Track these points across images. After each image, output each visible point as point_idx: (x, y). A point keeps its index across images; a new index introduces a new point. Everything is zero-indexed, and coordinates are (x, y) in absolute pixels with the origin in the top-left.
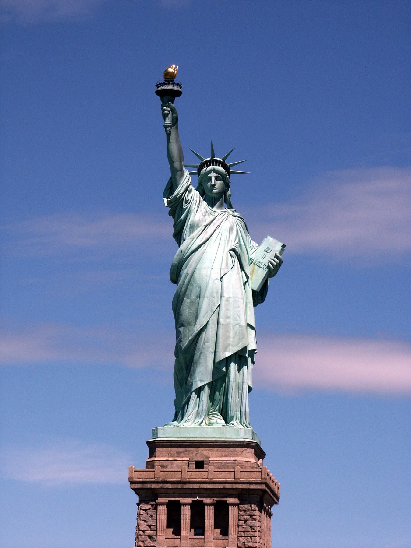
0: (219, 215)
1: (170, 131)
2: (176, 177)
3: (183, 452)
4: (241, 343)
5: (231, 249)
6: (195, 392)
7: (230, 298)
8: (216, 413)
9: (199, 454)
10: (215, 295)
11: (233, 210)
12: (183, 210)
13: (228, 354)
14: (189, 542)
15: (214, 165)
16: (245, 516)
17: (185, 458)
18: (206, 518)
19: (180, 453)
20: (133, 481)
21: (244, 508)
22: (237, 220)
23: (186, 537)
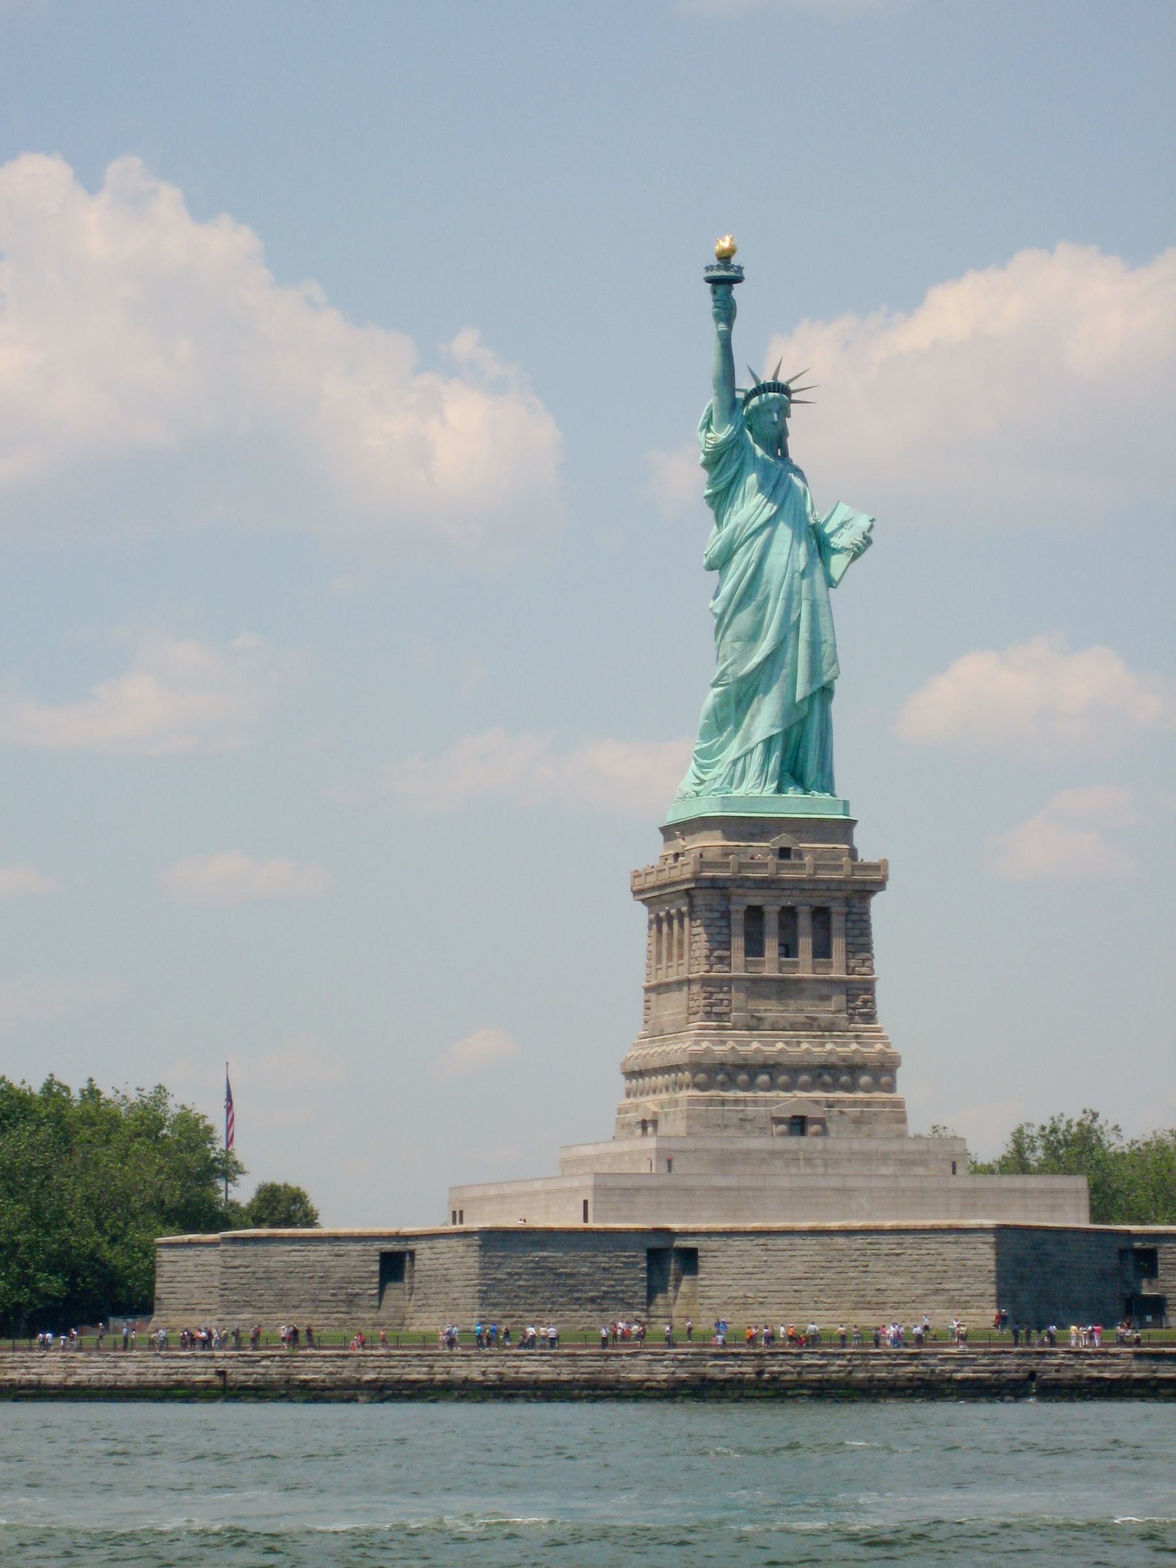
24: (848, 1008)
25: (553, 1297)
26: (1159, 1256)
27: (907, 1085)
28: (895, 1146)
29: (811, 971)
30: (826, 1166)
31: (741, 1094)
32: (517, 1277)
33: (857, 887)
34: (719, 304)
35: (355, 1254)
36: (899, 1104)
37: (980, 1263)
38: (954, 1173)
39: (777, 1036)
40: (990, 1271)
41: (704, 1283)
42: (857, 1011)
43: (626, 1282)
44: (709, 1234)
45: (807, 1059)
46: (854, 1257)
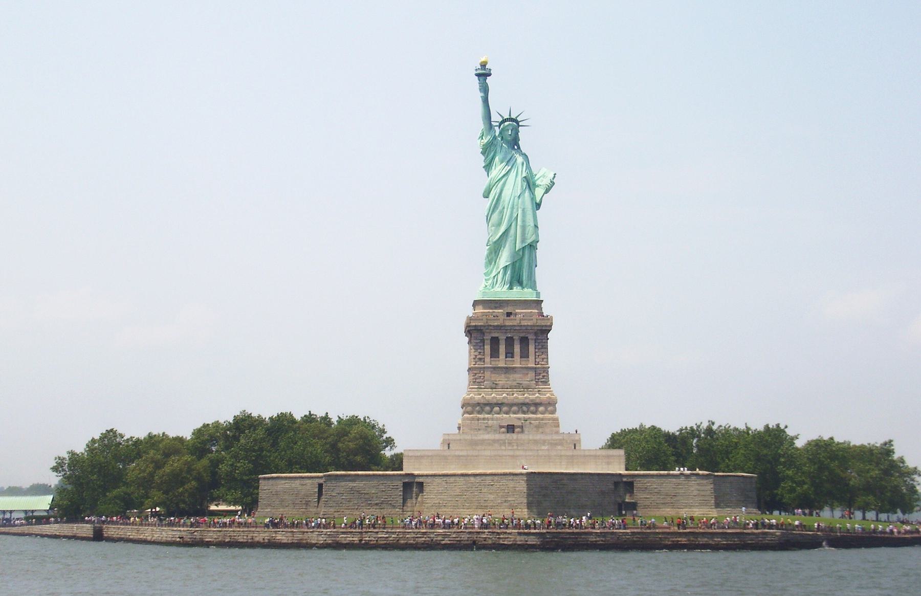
9: (509, 309)
12: (490, 152)
24: (536, 379)
25: (358, 503)
26: (635, 484)
27: (561, 412)
28: (555, 437)
29: (519, 363)
30: (517, 446)
31: (487, 416)
32: (341, 495)
33: (539, 328)
34: (481, 85)
35: (309, 484)
36: (557, 419)
37: (521, 489)
38: (575, 448)
39: (503, 391)
40: (524, 493)
41: (425, 497)
42: (540, 380)
43: (392, 497)
44: (427, 476)
45: (516, 401)
46: (477, 486)
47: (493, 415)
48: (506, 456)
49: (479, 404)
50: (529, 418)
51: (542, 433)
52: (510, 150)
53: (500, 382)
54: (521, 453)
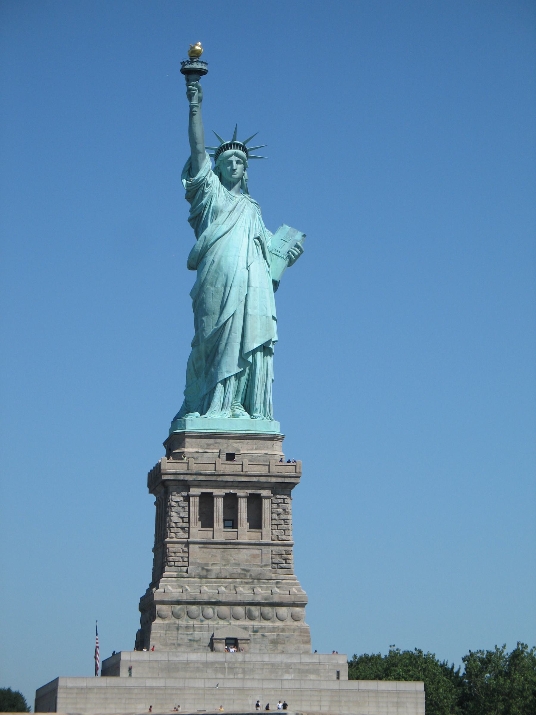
0: (240, 201)
1: (196, 111)
2: (198, 159)
3: (213, 444)
4: (268, 334)
5: (256, 237)
6: (220, 383)
7: (257, 287)
8: (239, 405)
9: (230, 448)
10: (242, 285)
11: (249, 196)
12: (203, 194)
13: (256, 345)
14: (222, 535)
15: (235, 149)
16: (277, 509)
17: (216, 450)
18: (239, 511)
19: (210, 445)
20: (166, 472)
21: (278, 501)
22: (255, 207)
23: (220, 529)
24: (272, 563)
30: (244, 672)
31: (191, 622)
33: (279, 480)
38: (338, 678)
45: (239, 599)
47: (202, 621)
48: (230, 689)
49: (179, 603)
50: (262, 628)
51: (283, 652)
52: (234, 194)
53: (214, 567)
54: (255, 684)
